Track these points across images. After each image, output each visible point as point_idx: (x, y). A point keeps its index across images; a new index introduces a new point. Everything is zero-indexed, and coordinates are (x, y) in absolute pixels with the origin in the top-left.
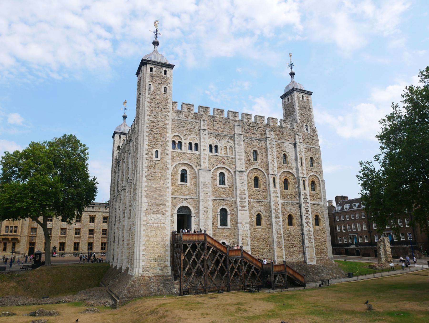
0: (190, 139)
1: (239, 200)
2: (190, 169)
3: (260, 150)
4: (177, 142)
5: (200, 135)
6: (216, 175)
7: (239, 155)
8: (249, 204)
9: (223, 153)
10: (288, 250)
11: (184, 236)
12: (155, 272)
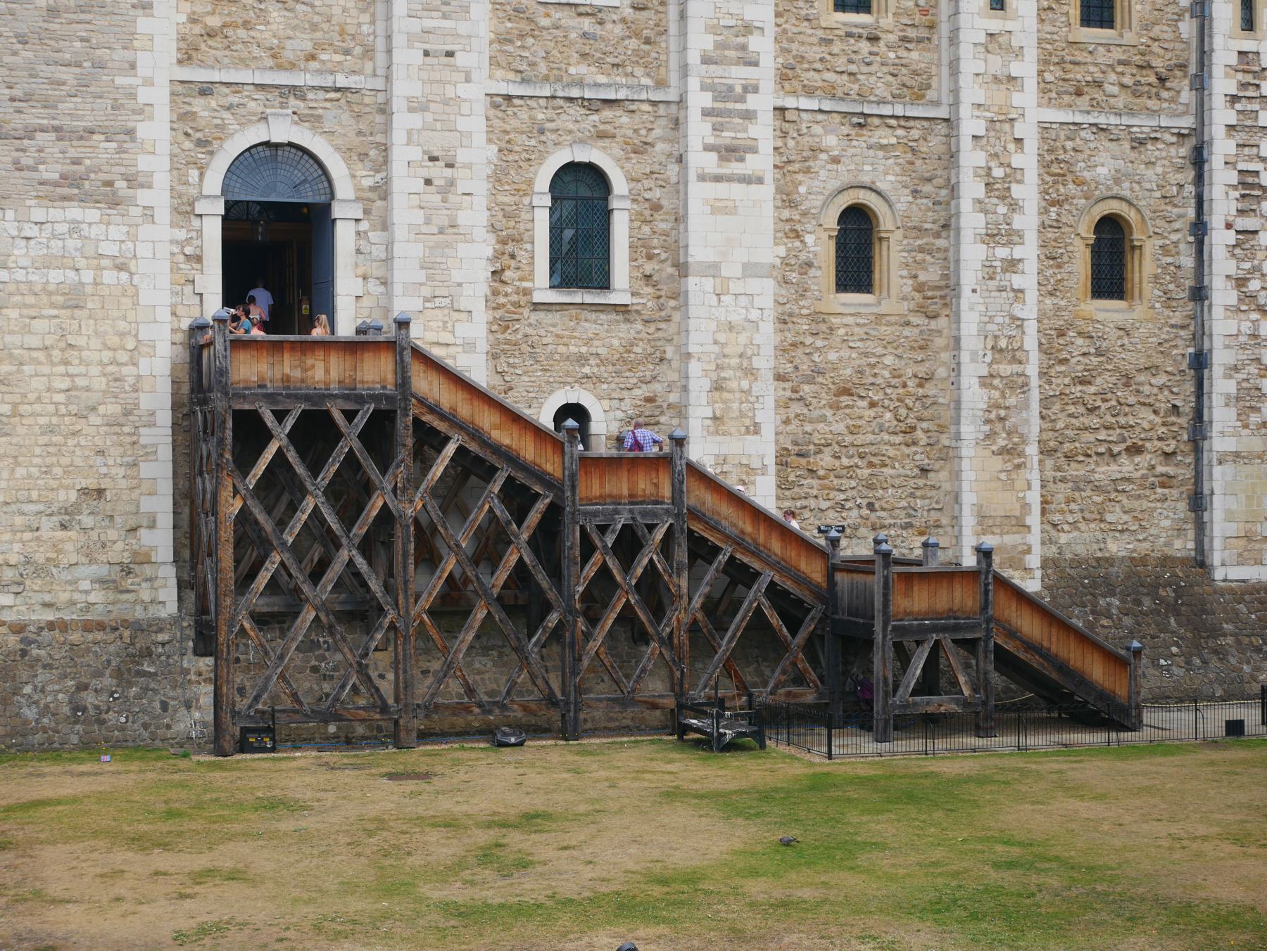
1: (699, 100)
8: (784, 135)
10: (1075, 471)
11: (243, 356)
12: (64, 597)
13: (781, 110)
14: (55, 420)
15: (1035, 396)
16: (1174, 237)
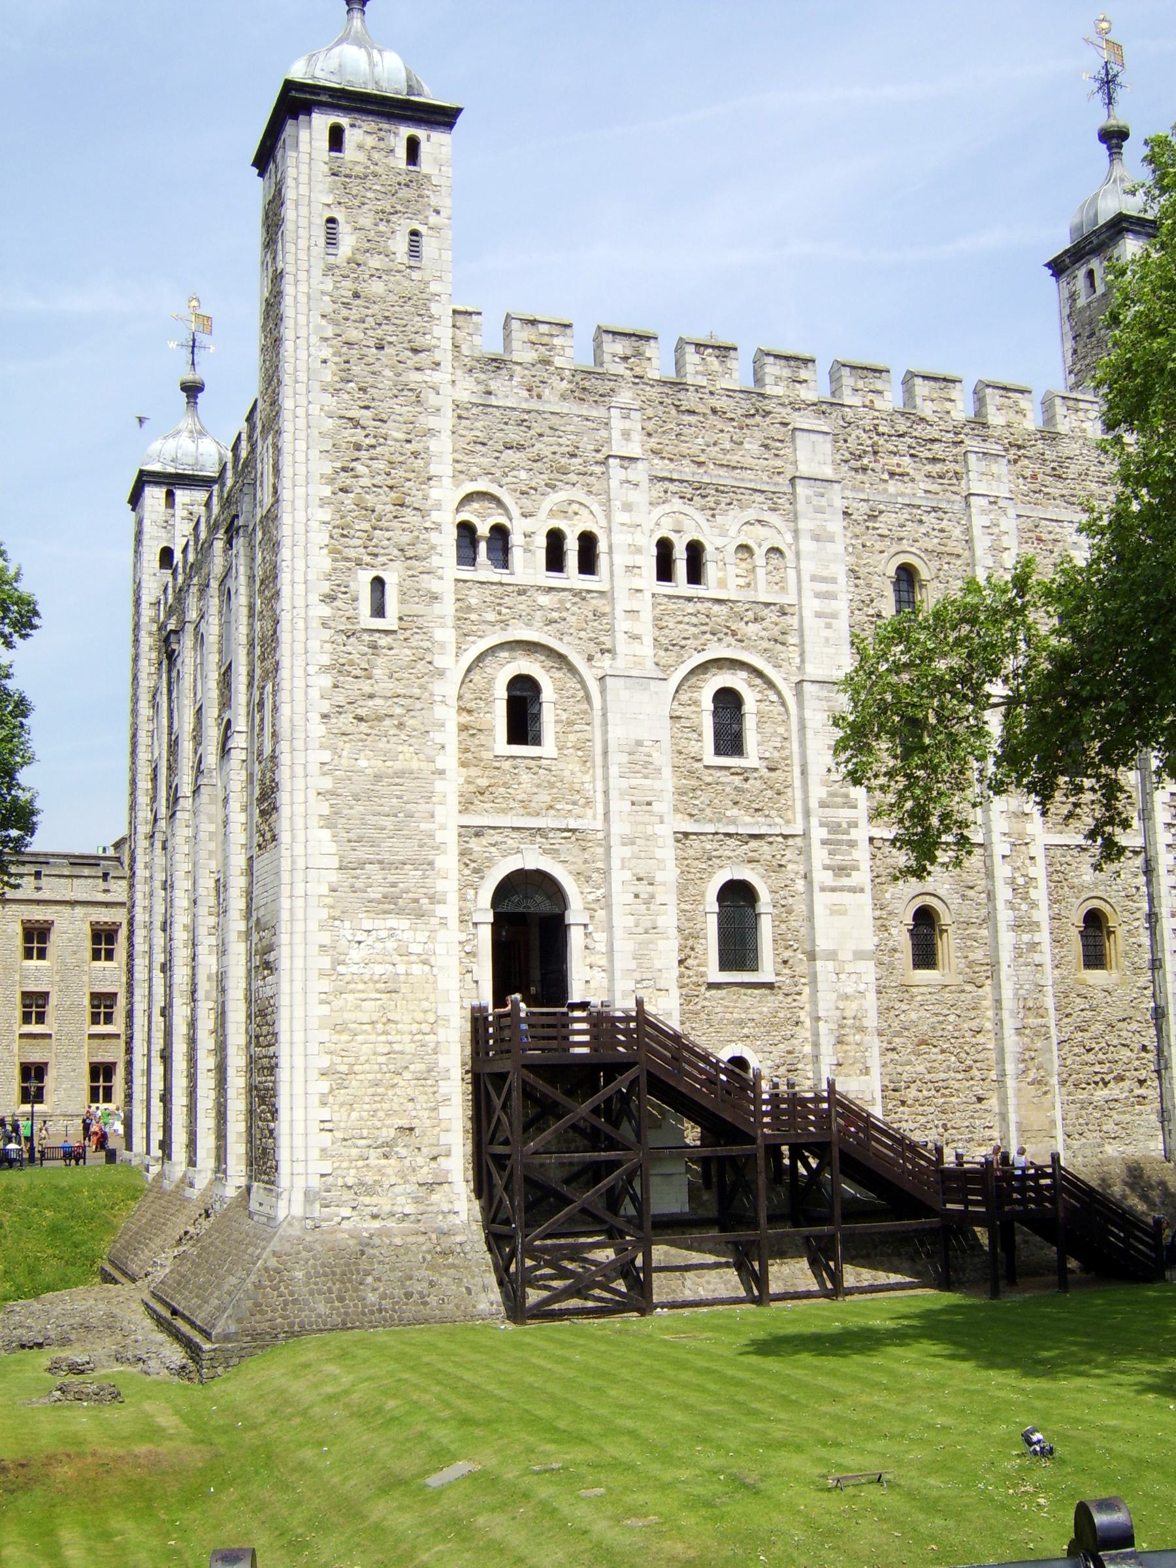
0: (552, 514)
1: (819, 833)
2: (558, 675)
3: (935, 564)
4: (483, 529)
5: (608, 492)
6: (696, 703)
7: (818, 595)
9: (733, 582)
10: (1082, 1096)
12: (387, 1208)
13: (871, 839)
14: (379, 1076)
15: (1055, 1041)
16: (1136, 924)
